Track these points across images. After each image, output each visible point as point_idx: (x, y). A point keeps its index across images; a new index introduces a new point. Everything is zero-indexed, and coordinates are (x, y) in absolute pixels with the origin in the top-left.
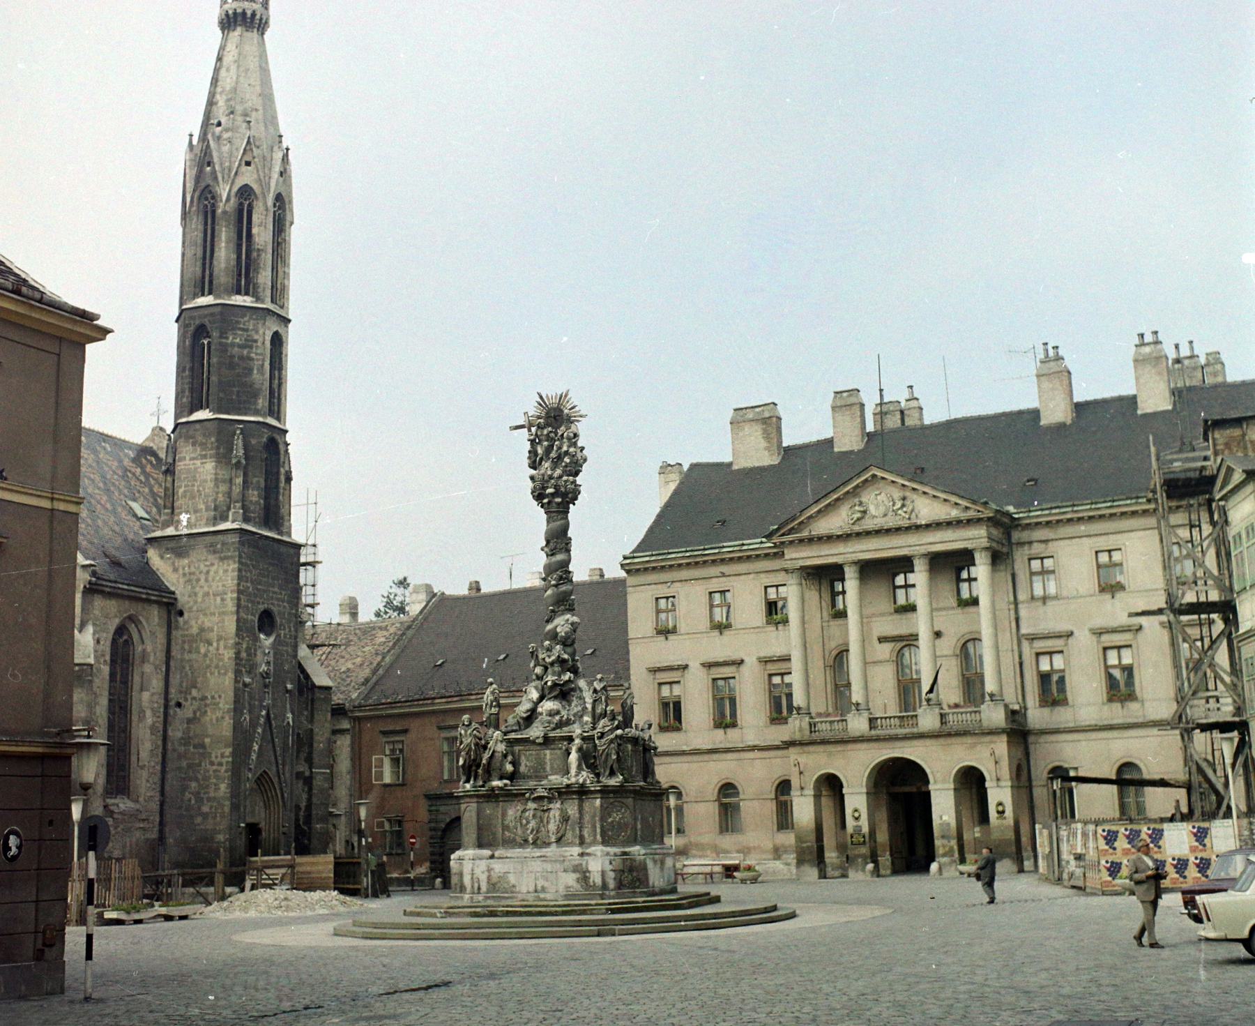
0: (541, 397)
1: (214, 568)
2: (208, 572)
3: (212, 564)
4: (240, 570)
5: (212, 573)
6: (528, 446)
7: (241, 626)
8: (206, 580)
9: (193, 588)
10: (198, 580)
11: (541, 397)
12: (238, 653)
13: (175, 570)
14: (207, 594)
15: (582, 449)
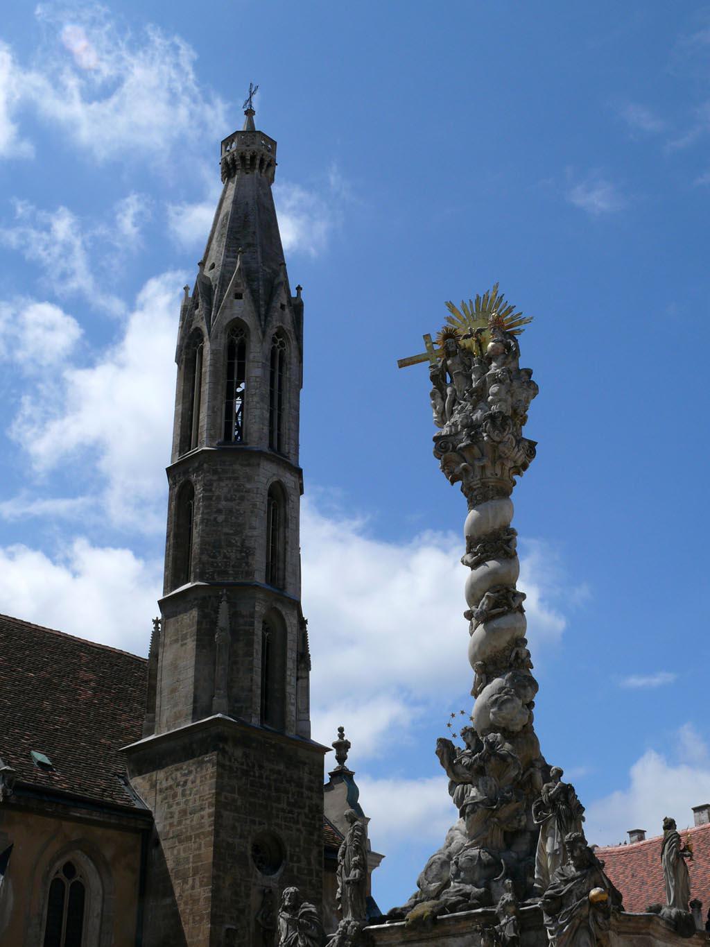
0: (451, 306)
1: (191, 777)
2: (185, 782)
3: (190, 772)
4: (219, 776)
5: (189, 785)
6: (430, 386)
7: (221, 851)
8: (183, 795)
9: (170, 807)
10: (175, 796)
11: (451, 306)
12: (216, 893)
13: (153, 786)
14: (184, 813)
15: (529, 372)
